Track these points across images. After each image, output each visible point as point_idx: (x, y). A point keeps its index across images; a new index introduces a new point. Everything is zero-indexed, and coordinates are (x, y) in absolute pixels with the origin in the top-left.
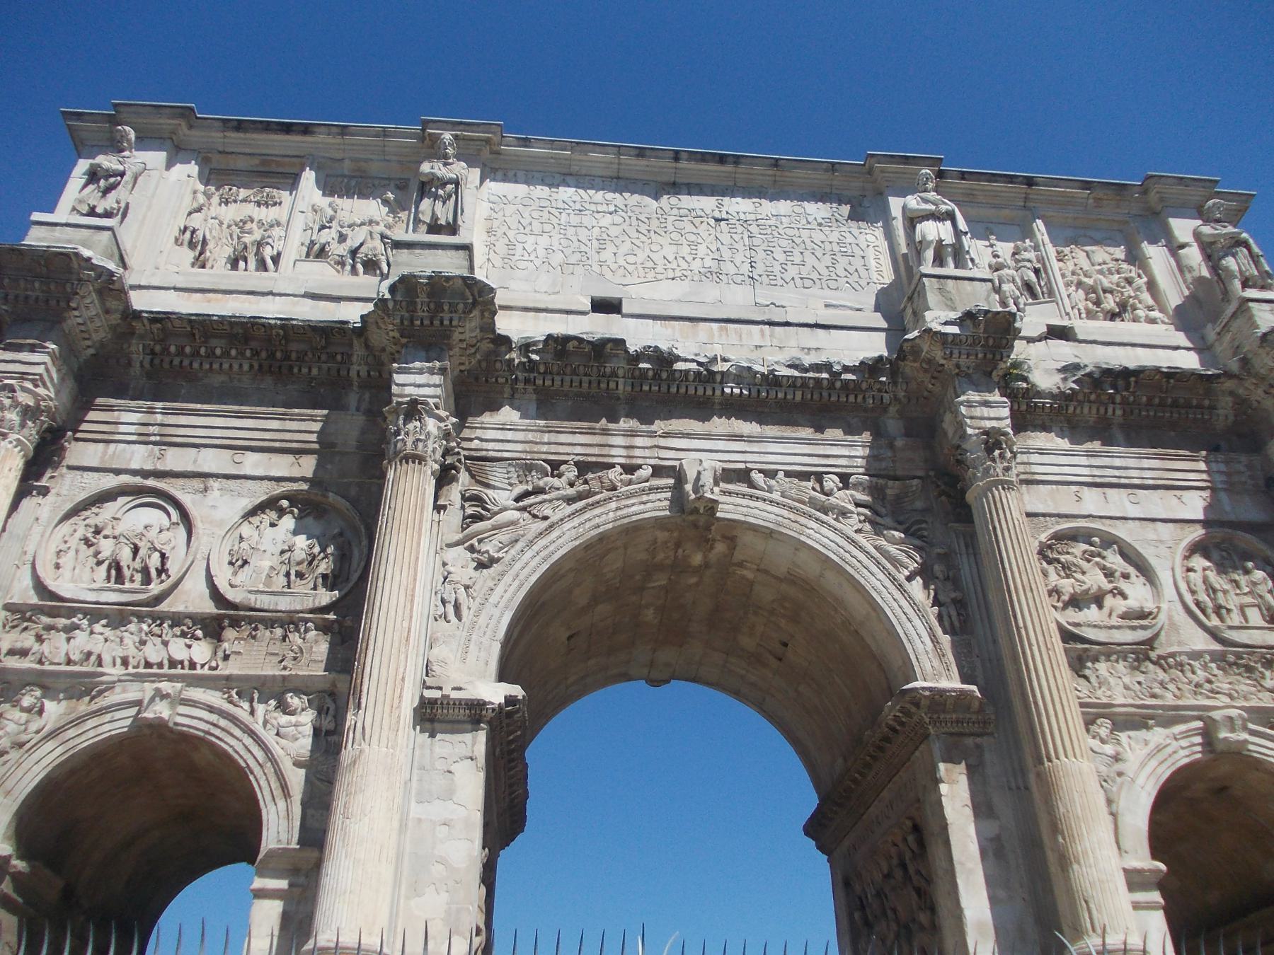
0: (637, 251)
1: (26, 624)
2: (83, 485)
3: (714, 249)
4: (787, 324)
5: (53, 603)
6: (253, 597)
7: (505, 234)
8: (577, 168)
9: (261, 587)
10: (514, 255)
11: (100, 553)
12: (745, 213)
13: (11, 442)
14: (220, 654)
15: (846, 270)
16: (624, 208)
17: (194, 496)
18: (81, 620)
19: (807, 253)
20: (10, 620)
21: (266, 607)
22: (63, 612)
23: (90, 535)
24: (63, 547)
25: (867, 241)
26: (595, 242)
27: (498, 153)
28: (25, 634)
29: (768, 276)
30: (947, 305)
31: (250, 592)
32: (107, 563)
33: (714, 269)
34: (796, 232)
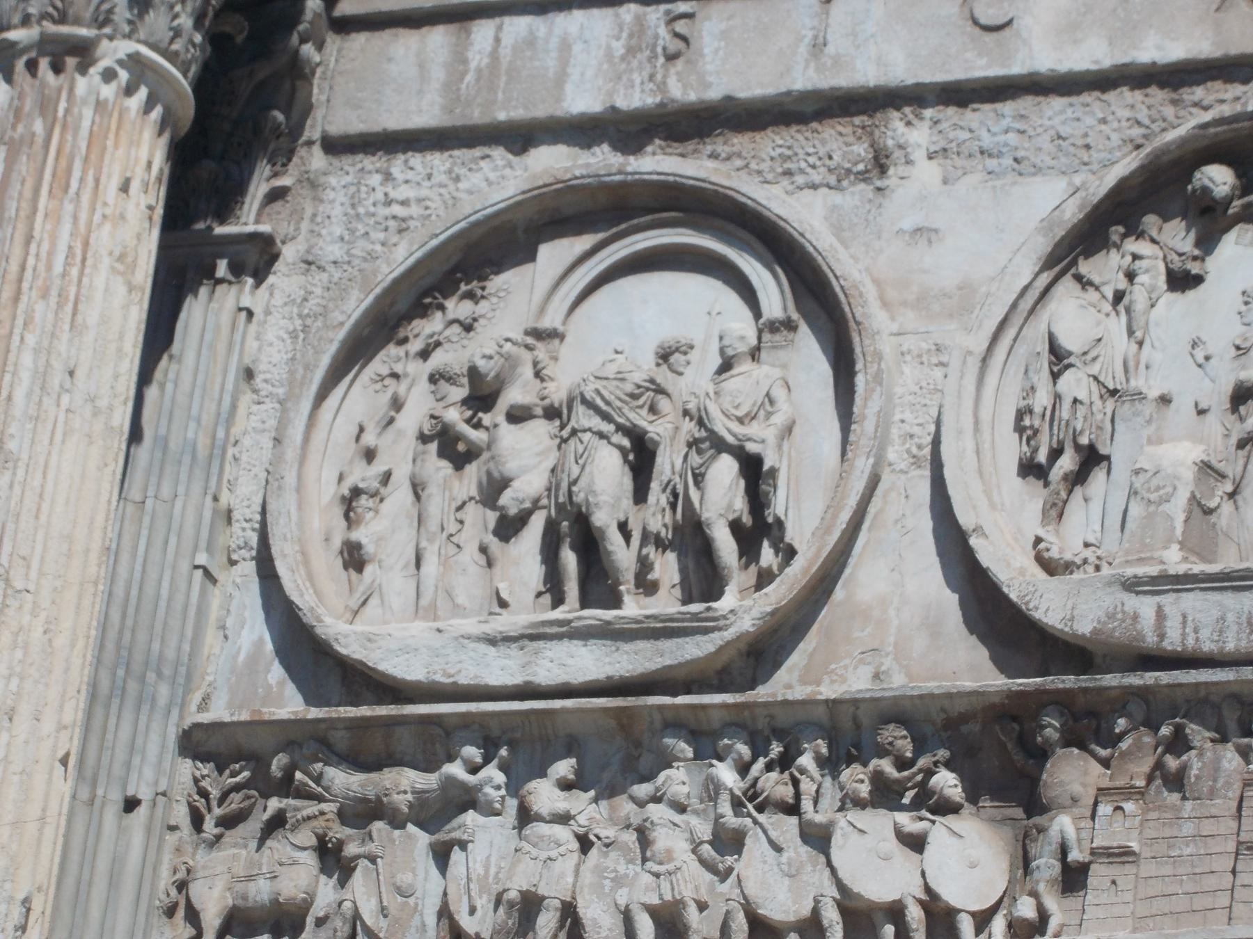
1: (274, 804)
2: (397, 210)
5: (365, 711)
6: (1145, 607)
9: (1174, 560)
11: (504, 483)
13: (109, 75)
14: (1047, 866)
17: (836, 198)
18: (474, 770)
20: (215, 793)
21: (1208, 647)
22: (405, 740)
23: (454, 416)
24: (362, 475)
28: (278, 846)
31: (1132, 585)
32: (537, 524)
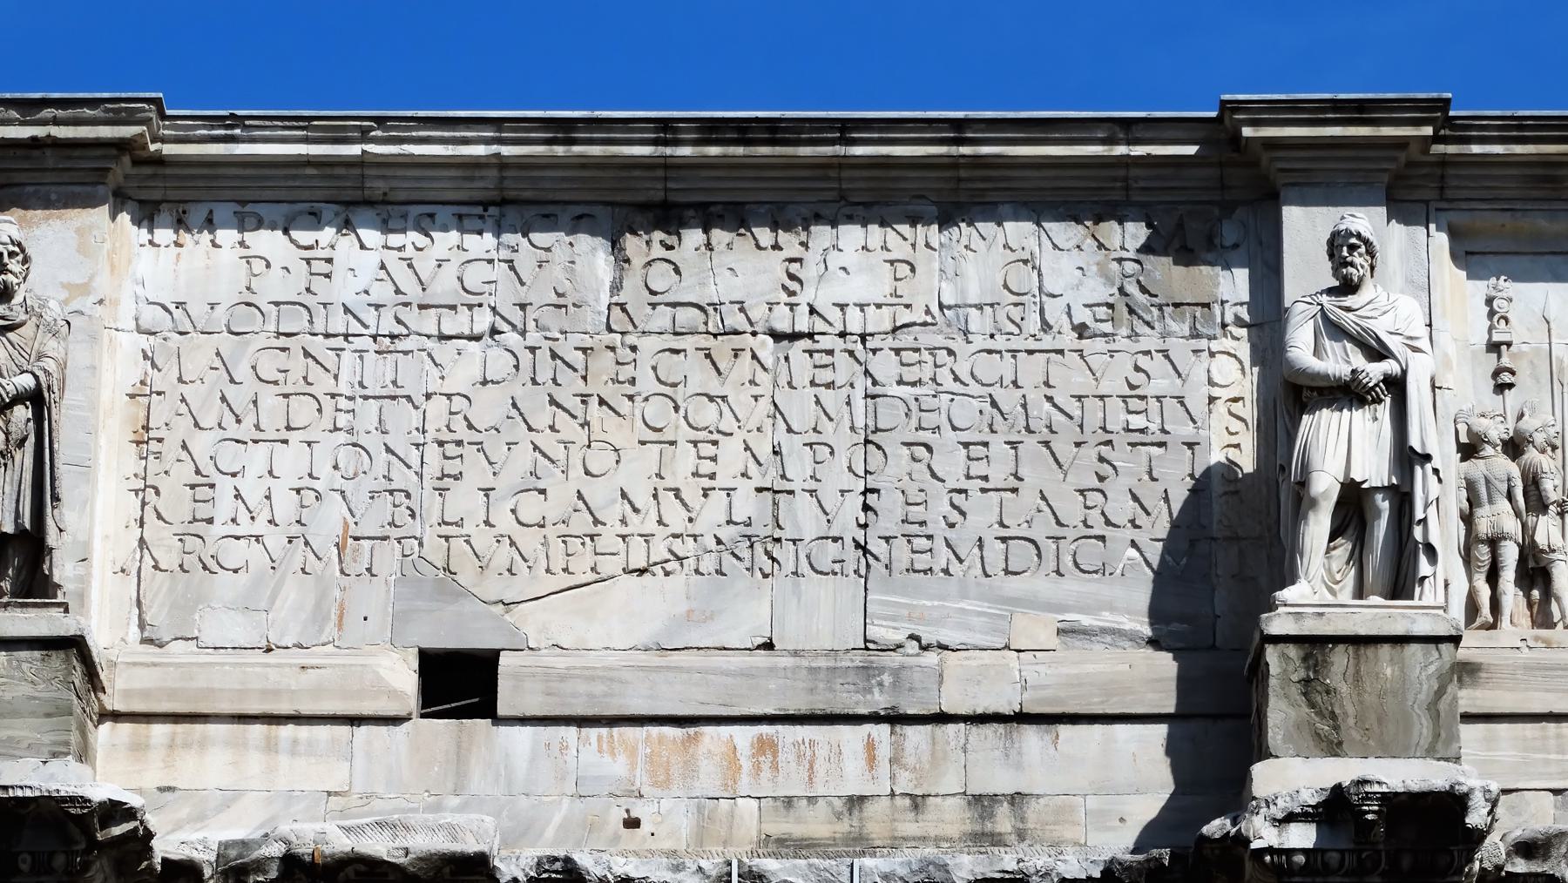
0: (551, 479)
3: (764, 451)
4: (942, 718)
7: (184, 447)
8: (381, 186)
10: (210, 521)
12: (862, 307)
15: (1135, 498)
16: (516, 316)
19: (1030, 444)
25: (1211, 383)
26: (432, 452)
27: (159, 161)
29: (909, 537)
30: (1317, 735)
33: (758, 530)
34: (1005, 367)
